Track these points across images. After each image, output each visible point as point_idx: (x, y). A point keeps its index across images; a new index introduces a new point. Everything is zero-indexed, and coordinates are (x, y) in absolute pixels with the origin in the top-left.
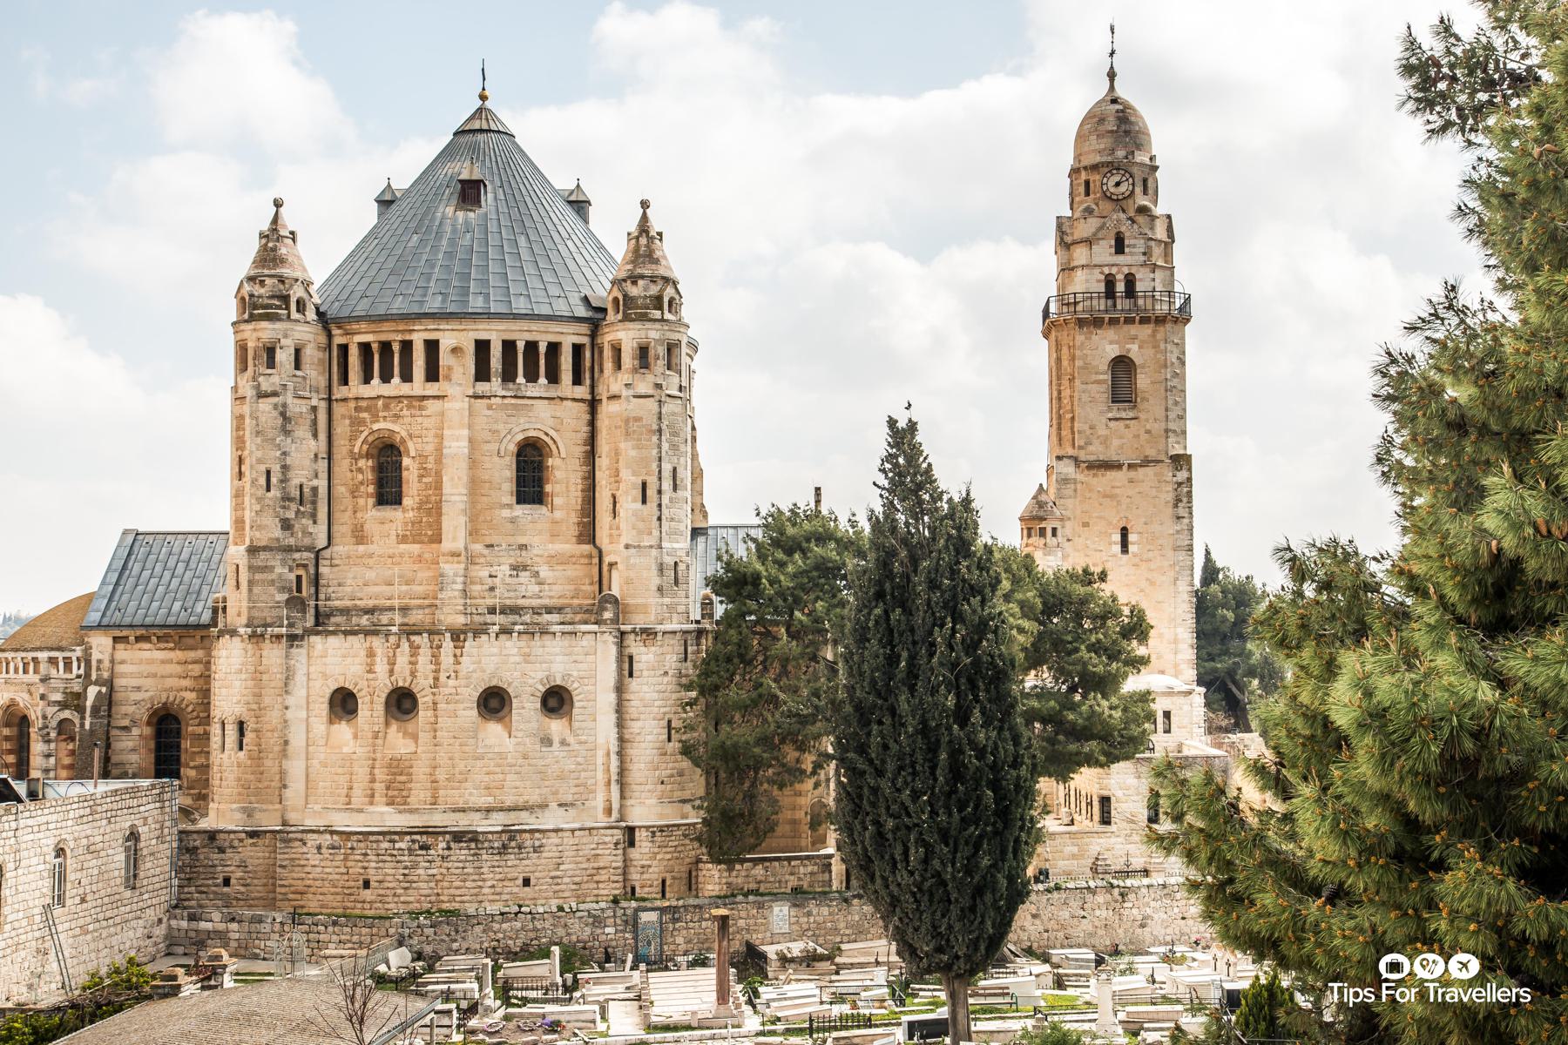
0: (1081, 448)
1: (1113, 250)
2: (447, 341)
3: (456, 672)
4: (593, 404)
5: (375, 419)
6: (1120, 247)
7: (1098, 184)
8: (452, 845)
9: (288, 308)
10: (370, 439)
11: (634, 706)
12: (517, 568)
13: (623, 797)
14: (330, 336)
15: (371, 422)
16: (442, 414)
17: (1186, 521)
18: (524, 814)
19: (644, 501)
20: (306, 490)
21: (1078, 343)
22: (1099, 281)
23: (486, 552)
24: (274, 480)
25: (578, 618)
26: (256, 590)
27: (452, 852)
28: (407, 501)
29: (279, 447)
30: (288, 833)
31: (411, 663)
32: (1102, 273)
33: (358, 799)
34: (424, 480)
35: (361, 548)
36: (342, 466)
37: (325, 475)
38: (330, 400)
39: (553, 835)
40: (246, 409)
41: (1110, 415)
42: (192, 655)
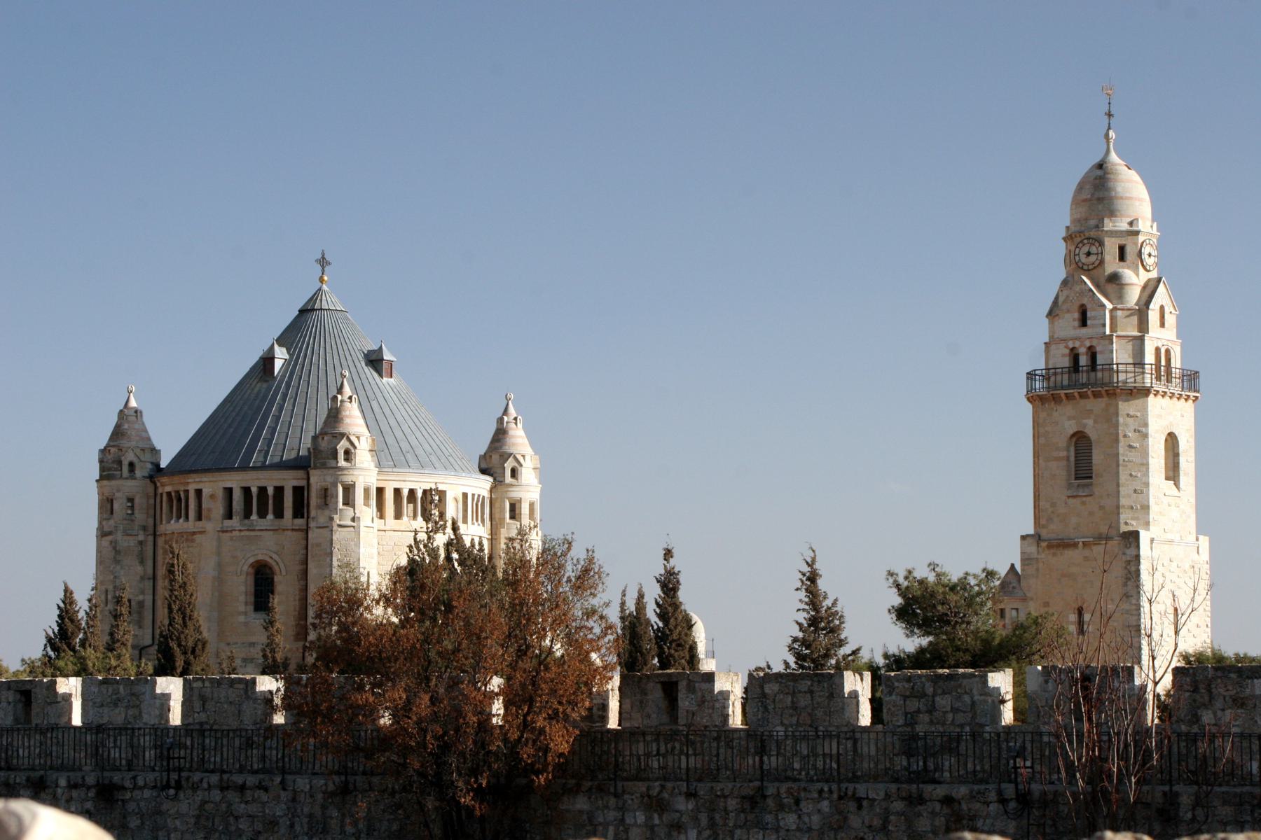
1: (1076, 324)
2: (206, 492)
4: (306, 531)
6: (1084, 322)
9: (121, 470)
14: (156, 488)
22: (1063, 355)
32: (1066, 347)
38: (155, 535)
41: (1070, 493)
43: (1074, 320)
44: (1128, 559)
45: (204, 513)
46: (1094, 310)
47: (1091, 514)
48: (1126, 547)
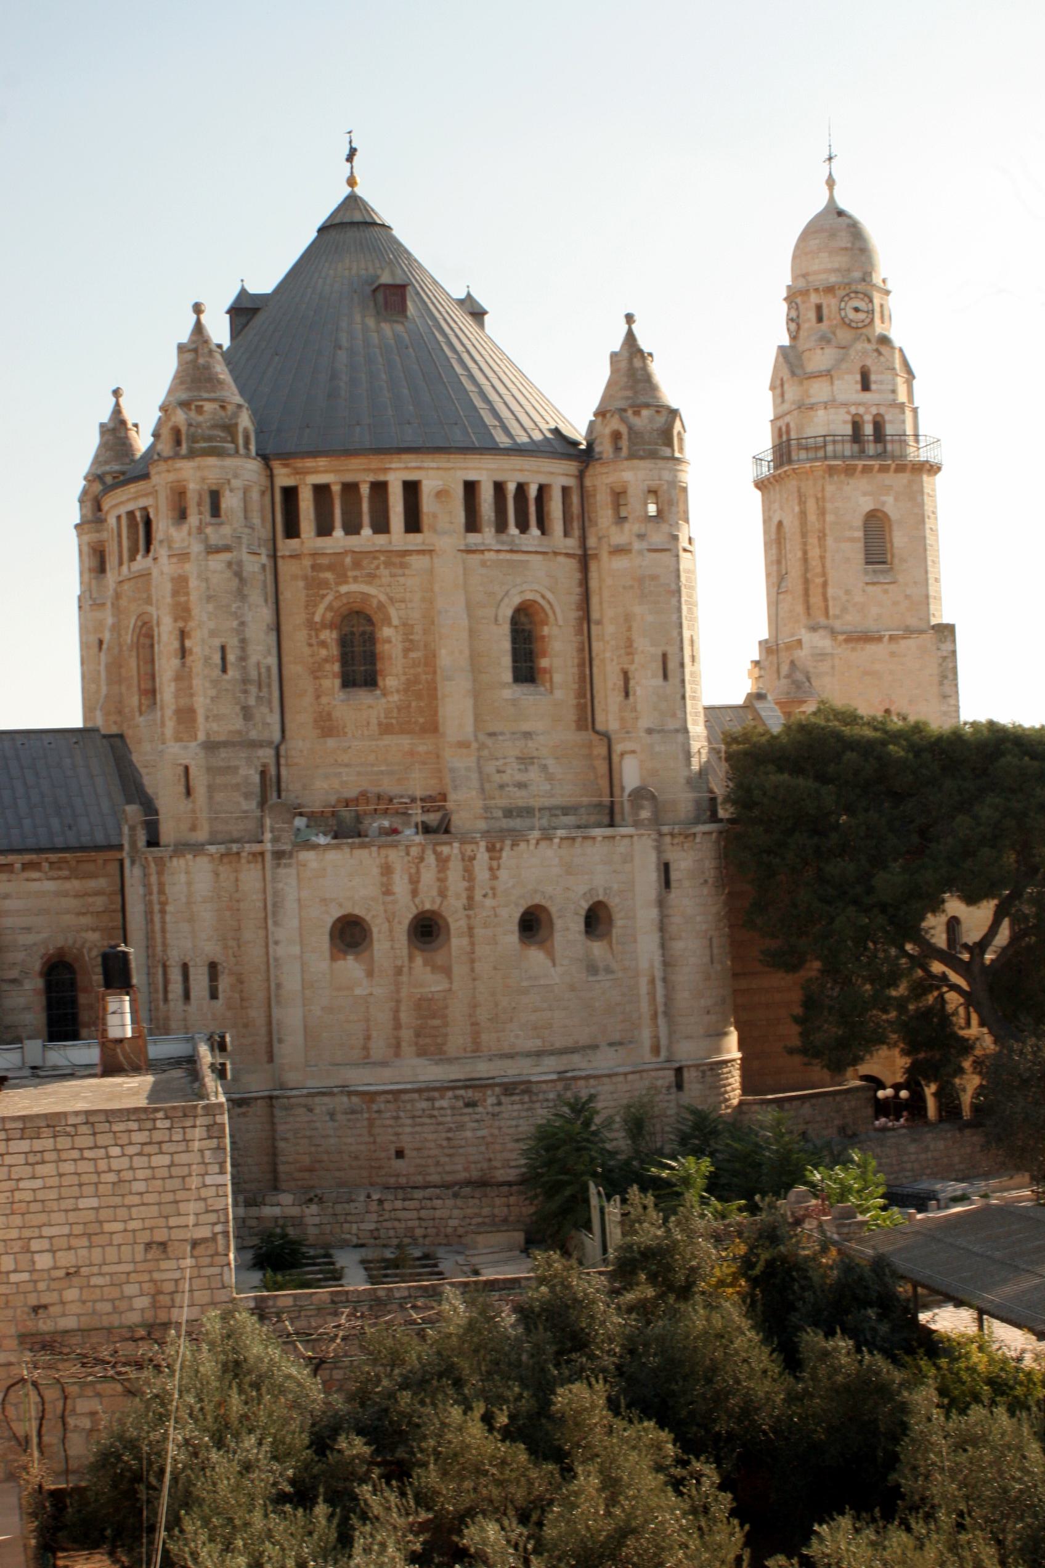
0: (837, 617)
1: (859, 387)
2: (429, 487)
3: (493, 889)
4: (584, 560)
5: (343, 579)
6: (866, 386)
7: (834, 309)
8: (504, 1099)
9: (234, 441)
10: (336, 604)
11: (676, 920)
12: (526, 761)
13: (671, 1034)
14: (271, 477)
15: (338, 584)
16: (431, 571)
17: (952, 702)
18: (576, 1058)
19: (665, 677)
20: (263, 670)
21: (828, 495)
22: (845, 422)
23: (489, 742)
24: (231, 657)
25: (593, 819)
26: (219, 797)
27: (503, 1108)
28: (392, 680)
29: (235, 615)
30: (288, 1098)
31: (439, 880)
32: (848, 413)
33: (379, 1048)
34: (413, 655)
35: (331, 743)
36: (297, 639)
37: (274, 651)
38: (274, 556)
39: (606, 1080)
40: (190, 568)
41: (868, 579)
42: (92, 884)
43: (856, 382)
44: (945, 654)
45: (426, 521)
46: (882, 373)
47: (895, 603)
48: (940, 641)
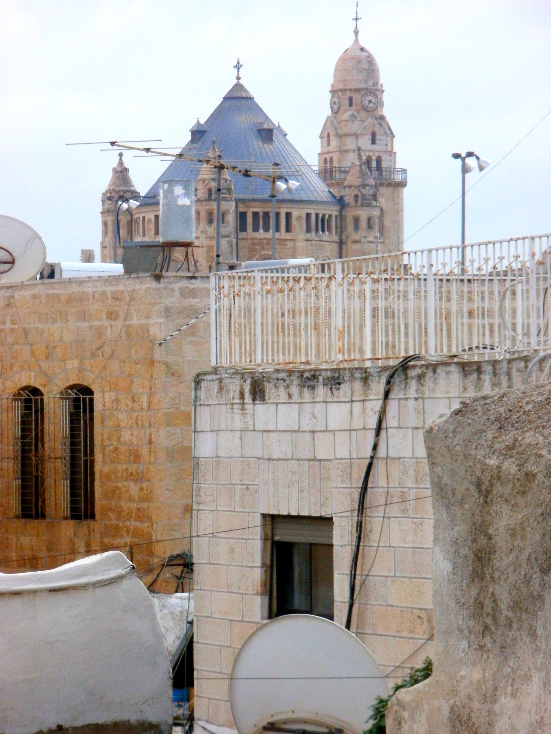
1: (370, 142)
2: (295, 213)
5: (263, 249)
6: (374, 142)
7: (359, 100)
38: (237, 239)
